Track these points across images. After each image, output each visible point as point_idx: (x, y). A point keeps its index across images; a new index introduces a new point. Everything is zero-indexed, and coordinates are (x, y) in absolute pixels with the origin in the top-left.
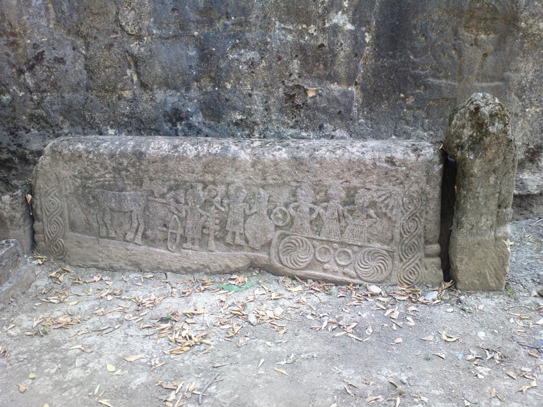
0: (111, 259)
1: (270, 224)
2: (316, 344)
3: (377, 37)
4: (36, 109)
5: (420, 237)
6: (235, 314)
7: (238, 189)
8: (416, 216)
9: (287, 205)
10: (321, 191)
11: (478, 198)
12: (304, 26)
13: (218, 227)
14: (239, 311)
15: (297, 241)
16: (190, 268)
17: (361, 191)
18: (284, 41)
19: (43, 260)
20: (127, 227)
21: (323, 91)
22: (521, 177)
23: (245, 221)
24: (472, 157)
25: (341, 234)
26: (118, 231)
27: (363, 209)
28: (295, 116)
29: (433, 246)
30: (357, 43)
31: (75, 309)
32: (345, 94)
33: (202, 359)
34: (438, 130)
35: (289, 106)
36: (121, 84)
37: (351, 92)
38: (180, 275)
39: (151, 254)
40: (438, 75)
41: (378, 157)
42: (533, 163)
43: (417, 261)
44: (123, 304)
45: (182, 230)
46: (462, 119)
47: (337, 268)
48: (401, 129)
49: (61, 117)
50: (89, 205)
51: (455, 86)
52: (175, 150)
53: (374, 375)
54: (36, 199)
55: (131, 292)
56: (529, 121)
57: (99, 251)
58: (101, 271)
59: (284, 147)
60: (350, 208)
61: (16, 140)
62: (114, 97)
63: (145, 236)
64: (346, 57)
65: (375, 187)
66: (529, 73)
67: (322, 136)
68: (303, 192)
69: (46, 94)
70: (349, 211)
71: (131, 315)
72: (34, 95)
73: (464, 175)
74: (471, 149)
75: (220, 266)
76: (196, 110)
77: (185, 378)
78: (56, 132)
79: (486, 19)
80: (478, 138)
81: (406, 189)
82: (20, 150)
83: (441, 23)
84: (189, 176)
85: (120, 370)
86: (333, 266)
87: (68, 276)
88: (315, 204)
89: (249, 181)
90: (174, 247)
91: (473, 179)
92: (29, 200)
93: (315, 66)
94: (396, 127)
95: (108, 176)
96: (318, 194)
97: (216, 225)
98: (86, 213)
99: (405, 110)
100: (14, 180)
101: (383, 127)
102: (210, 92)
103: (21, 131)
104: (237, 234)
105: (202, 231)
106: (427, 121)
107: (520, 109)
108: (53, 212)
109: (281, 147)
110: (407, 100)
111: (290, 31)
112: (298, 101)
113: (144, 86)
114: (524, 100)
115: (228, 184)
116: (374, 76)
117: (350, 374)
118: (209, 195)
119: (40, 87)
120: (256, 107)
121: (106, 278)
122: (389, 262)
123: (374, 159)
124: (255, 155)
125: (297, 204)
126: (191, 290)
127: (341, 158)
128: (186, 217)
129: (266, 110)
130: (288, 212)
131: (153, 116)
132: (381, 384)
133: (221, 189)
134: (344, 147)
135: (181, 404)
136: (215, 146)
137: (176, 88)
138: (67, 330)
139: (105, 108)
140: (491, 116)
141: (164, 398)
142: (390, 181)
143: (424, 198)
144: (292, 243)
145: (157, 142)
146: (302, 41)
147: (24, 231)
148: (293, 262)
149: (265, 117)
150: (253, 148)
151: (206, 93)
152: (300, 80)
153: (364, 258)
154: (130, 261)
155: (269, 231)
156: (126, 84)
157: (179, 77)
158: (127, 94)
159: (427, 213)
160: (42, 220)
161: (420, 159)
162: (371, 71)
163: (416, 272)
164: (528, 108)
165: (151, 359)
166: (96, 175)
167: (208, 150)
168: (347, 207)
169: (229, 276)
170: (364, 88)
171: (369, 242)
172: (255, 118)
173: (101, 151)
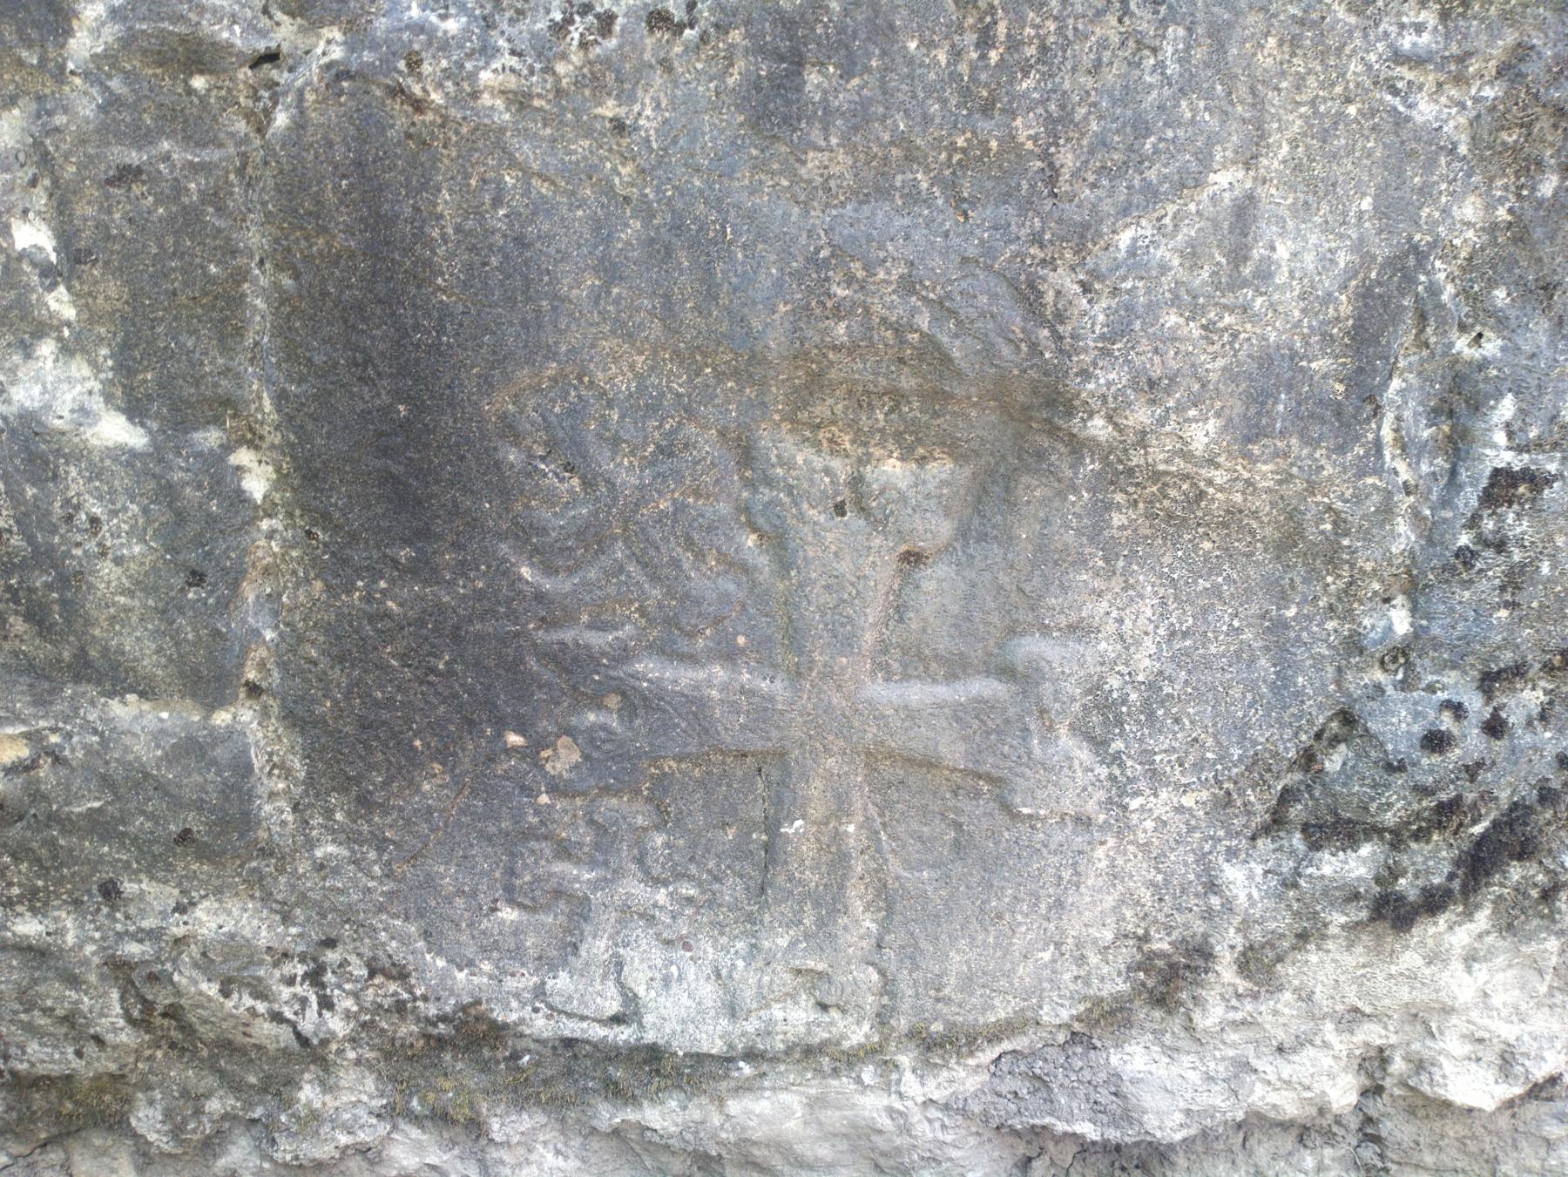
3: (305, 476)
30: (181, 518)
32: (192, 749)
34: (717, 879)
40: (683, 645)
42: (1169, 1013)
48: (537, 879)
51: (772, 699)
56: (1145, 847)
64: (141, 586)
66: (1138, 643)
79: (898, 397)
83: (652, 409)
94: (511, 872)
101: (448, 876)
106: (659, 840)
107: (1101, 795)
164: (1138, 793)
170: (300, 711)
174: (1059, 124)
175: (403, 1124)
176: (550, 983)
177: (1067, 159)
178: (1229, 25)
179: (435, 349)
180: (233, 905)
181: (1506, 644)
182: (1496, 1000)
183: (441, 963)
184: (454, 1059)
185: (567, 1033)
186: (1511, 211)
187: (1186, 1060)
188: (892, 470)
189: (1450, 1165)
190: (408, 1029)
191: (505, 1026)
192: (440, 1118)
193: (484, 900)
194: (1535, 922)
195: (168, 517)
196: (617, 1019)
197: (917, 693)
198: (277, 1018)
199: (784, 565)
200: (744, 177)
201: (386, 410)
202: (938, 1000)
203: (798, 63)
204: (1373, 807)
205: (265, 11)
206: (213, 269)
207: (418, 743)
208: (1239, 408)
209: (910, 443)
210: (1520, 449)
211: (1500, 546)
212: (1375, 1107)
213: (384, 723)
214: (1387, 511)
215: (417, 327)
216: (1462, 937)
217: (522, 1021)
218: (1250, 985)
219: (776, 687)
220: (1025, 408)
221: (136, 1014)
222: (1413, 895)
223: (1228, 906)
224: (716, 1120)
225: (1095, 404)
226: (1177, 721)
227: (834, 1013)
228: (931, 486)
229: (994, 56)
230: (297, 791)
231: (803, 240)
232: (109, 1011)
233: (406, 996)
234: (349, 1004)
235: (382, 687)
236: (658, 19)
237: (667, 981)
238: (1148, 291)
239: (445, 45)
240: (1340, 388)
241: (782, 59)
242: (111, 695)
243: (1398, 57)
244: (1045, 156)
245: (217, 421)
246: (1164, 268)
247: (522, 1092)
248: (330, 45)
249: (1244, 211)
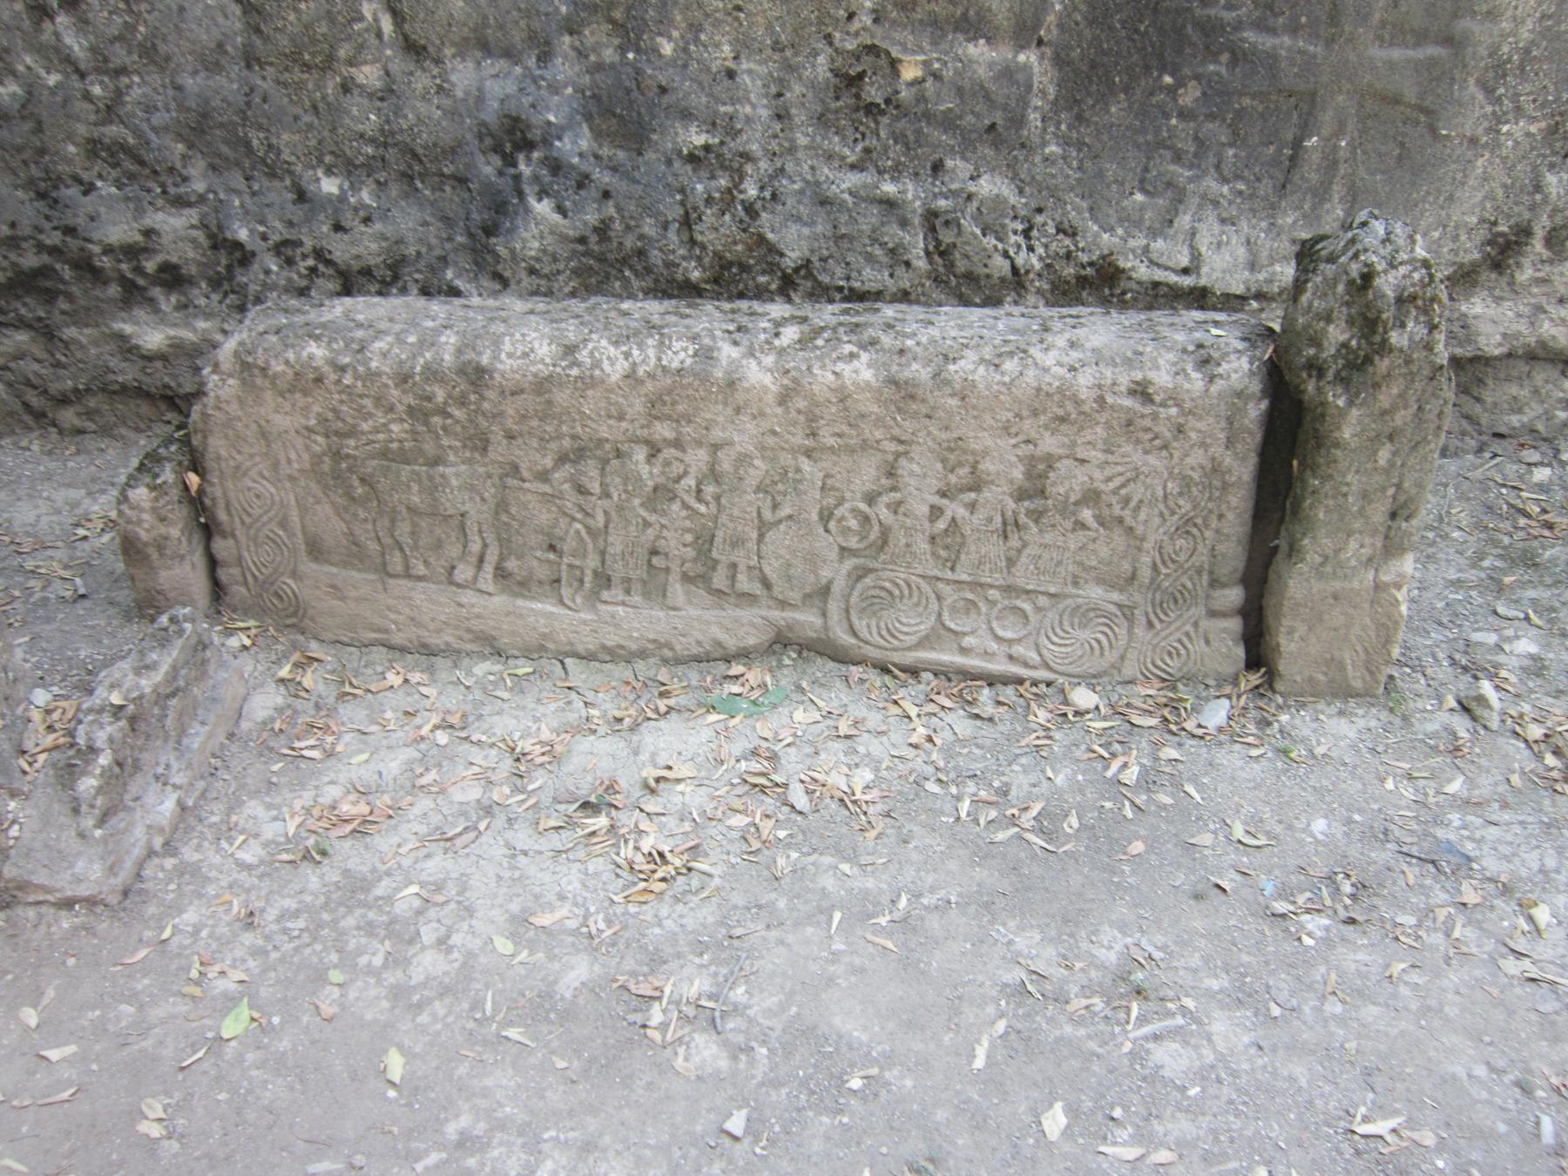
0: (419, 625)
1: (826, 545)
2: (952, 865)
4: (103, 123)
5: (1199, 572)
6: (756, 786)
7: (743, 459)
8: (1195, 525)
9: (871, 499)
10: (960, 464)
11: (1345, 495)
13: (690, 553)
14: (764, 775)
15: (897, 585)
16: (622, 647)
17: (1063, 466)
19: (254, 631)
20: (453, 550)
21: (946, 63)
23: (761, 536)
24: (1341, 403)
25: (1008, 567)
26: (432, 560)
27: (1066, 508)
28: (863, 135)
29: (1227, 592)
31: (367, 775)
32: (1008, 73)
33: (701, 915)
34: (1258, 180)
35: (847, 106)
36: (347, 46)
37: (1026, 67)
38: (597, 664)
39: (521, 616)
40: (1271, 22)
41: (1109, 382)
42: (1501, 274)
43: (1188, 628)
44: (477, 756)
45: (597, 558)
46: (1326, 295)
47: (993, 646)
48: (1160, 174)
49: (180, 146)
50: (353, 499)
51: (1315, 56)
52: (570, 358)
53: (1084, 945)
54: (212, 485)
55: (489, 720)
56: (1504, 159)
57: (389, 609)
58: (398, 654)
59: (863, 347)
60: (1032, 506)
61: (57, 214)
62: (330, 84)
63: (501, 574)
65: (1100, 455)
66: (1523, 22)
67: (941, 193)
68: (915, 467)
69: (127, 80)
70: (1029, 513)
71: (507, 790)
72: (92, 83)
73: (1320, 441)
74: (1342, 380)
75: (699, 643)
76: (571, 118)
77: (673, 965)
78: (172, 190)
80: (1362, 353)
81: (1176, 460)
82: (73, 244)
84: (610, 427)
85: (525, 953)
86: (984, 642)
87: (321, 671)
88: (944, 495)
89: (770, 441)
90: (579, 600)
91: (1338, 453)
92: (194, 489)
94: (1146, 170)
95: (395, 428)
96: (952, 471)
97: (685, 545)
98: (348, 517)
99: (1174, 121)
100: (68, 326)
101: (1111, 169)
102: (612, 66)
103: (67, 187)
104: (742, 567)
105: (649, 561)
106: (1231, 152)
107: (1486, 124)
108: (261, 516)
109: (855, 349)
110: (1181, 91)
112: (873, 92)
113: (414, 49)
115: (716, 448)
116: (1091, 23)
117: (1031, 944)
118: (663, 473)
119: (106, 60)
120: (748, 109)
121: (416, 677)
122: (1122, 632)
123: (1100, 387)
124: (787, 372)
125: (898, 495)
126: (632, 712)
127: (1017, 382)
128: (606, 527)
129: (779, 117)
130: (873, 516)
131: (447, 139)
132: (1097, 967)
133: (698, 458)
134: (1025, 351)
135: (679, 1033)
136: (677, 345)
137: (509, 54)
138: (368, 840)
139: (307, 118)
140: (1400, 300)
141: (638, 1018)
142: (1138, 441)
143: (1216, 483)
144: (882, 588)
145: (518, 336)
147: (193, 565)
148: (884, 633)
149: (776, 136)
150: (781, 352)
151: (599, 67)
152: (878, 31)
153: (1061, 623)
154: (469, 630)
155: (824, 561)
156: (361, 47)
157: (517, 23)
158: (368, 75)
159: (1221, 516)
160: (233, 536)
161: (1214, 389)
162: (1084, 8)
163: (1183, 652)
164: (1507, 122)
165: (586, 918)
166: (365, 426)
167: (659, 359)
168: (1026, 503)
169: (721, 668)
170: (1063, 55)
171: (1075, 584)
172: (747, 142)
173: (374, 364)
180: (998, 180)
183: (1096, 228)
185: (1156, 278)
190: (1069, 271)
191: (1123, 271)
193: (1127, 187)
197: (1396, 54)
198: (1006, 255)
217: (1133, 269)
219: (1316, 49)
221: (931, 248)
223: (1545, 200)
230: (1047, 108)
232: (916, 245)
234: (1041, 251)
237: (1219, 245)
242: (969, 40)
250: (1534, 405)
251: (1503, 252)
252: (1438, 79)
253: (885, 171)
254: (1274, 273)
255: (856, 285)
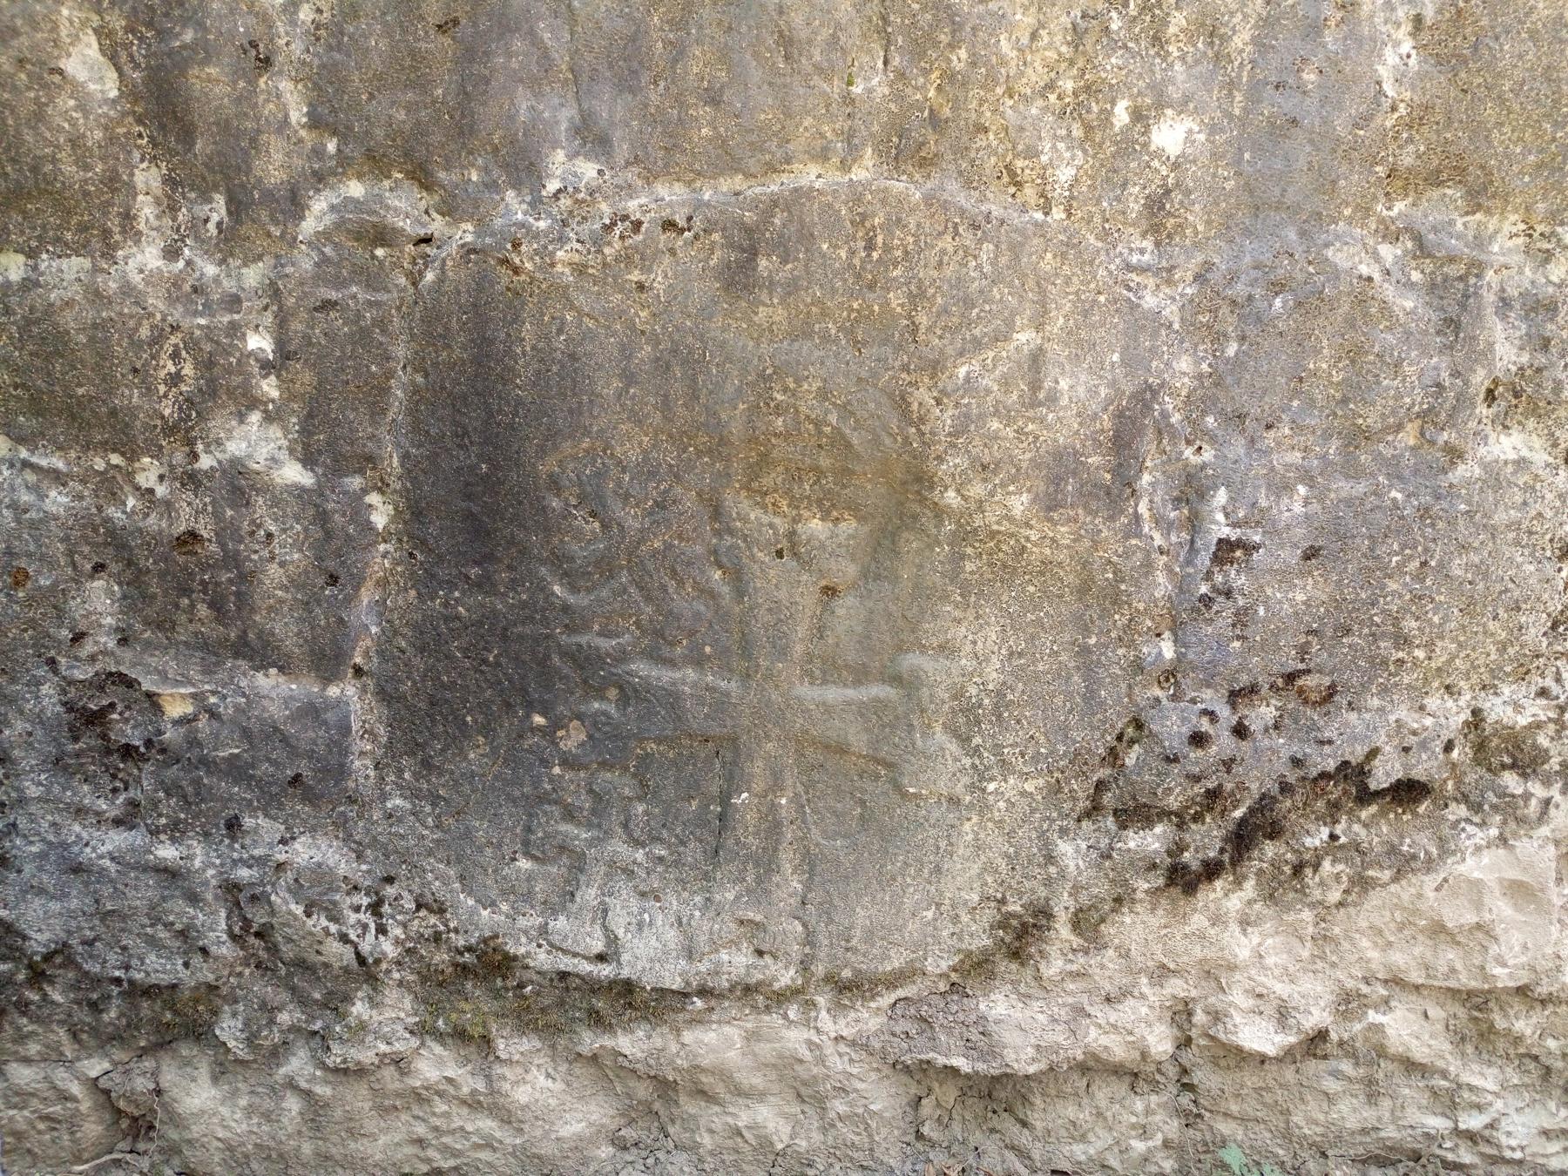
3: (413, 513)
12: (116, 459)
18: (33, 514)
22: (982, 1006)
30: (328, 535)
32: (311, 712)
34: (683, 843)
37: (340, 703)
40: (666, 651)
42: (1022, 964)
48: (547, 836)
51: (728, 695)
56: (1000, 823)
64: (294, 583)
66: (987, 660)
67: (241, 860)
79: (819, 472)
83: (652, 474)
93: (177, 606)
94: (529, 829)
99: (557, 770)
101: (481, 829)
106: (640, 808)
107: (966, 780)
110: (560, 733)
111: (57, 477)
114: (976, 751)
146: (113, 512)
152: (127, 654)
164: (992, 779)
170: (389, 688)
174: (917, 297)
175: (429, 1042)
176: (552, 924)
177: (923, 319)
178: (1022, 245)
179: (512, 427)
180: (323, 842)
181: (1243, 668)
182: (1270, 961)
183: (471, 902)
184: (477, 985)
185: (562, 967)
186: (1210, 365)
187: (1036, 1005)
188: (815, 526)
189: (1251, 1113)
190: (441, 957)
191: (515, 958)
192: (460, 1035)
194: (1291, 895)
195: (320, 535)
196: (601, 958)
197: (833, 694)
198: (344, 938)
199: (740, 593)
200: (718, 321)
201: (475, 467)
202: (847, 949)
203: (753, 253)
204: (1159, 791)
205: (427, 212)
206: (374, 368)
207: (469, 719)
208: (1042, 487)
209: (827, 507)
210: (1234, 525)
211: (1228, 594)
212: (1187, 1057)
213: (447, 701)
214: (1148, 566)
215: (500, 411)
216: (1235, 903)
217: (528, 954)
218: (1081, 941)
219: (733, 686)
220: (904, 483)
221: (237, 930)
222: (1195, 865)
223: (1062, 874)
224: (674, 1047)
225: (948, 480)
226: (1018, 722)
227: (767, 958)
228: (842, 539)
229: (875, 255)
231: (755, 362)
232: (216, 926)
233: (442, 928)
234: (398, 932)
235: (448, 673)
236: (669, 225)
237: (640, 925)
238: (979, 406)
239: (536, 236)
240: (1108, 476)
241: (744, 251)
243: (1130, 268)
244: (910, 317)
245: (361, 471)
246: (988, 391)
247: (526, 1019)
248: (466, 233)
249: (1037, 358)
250: (1101, 1132)
251: (1021, 936)
252: (893, 727)
253: (158, 832)
254: (719, 963)
255: (138, 976)
